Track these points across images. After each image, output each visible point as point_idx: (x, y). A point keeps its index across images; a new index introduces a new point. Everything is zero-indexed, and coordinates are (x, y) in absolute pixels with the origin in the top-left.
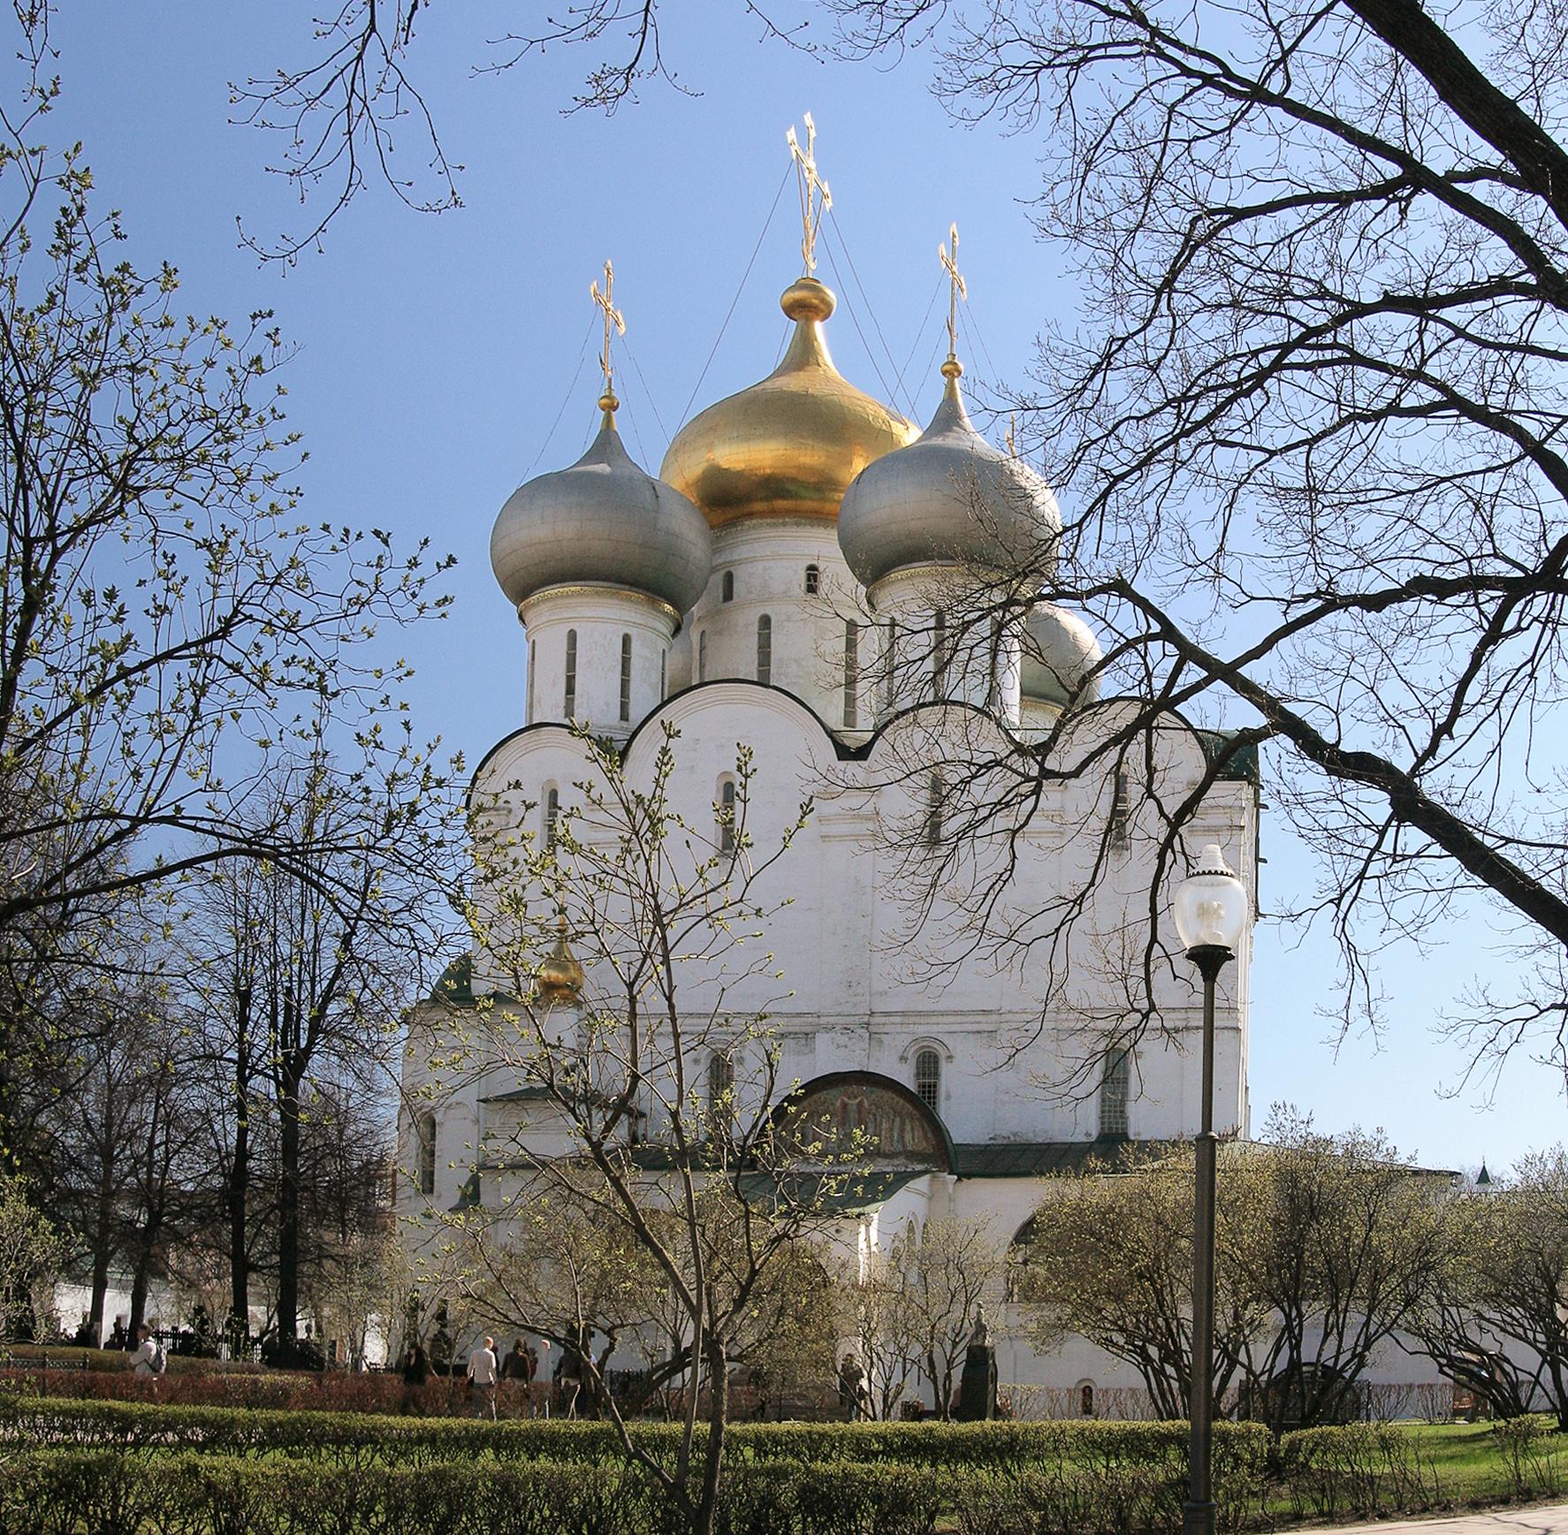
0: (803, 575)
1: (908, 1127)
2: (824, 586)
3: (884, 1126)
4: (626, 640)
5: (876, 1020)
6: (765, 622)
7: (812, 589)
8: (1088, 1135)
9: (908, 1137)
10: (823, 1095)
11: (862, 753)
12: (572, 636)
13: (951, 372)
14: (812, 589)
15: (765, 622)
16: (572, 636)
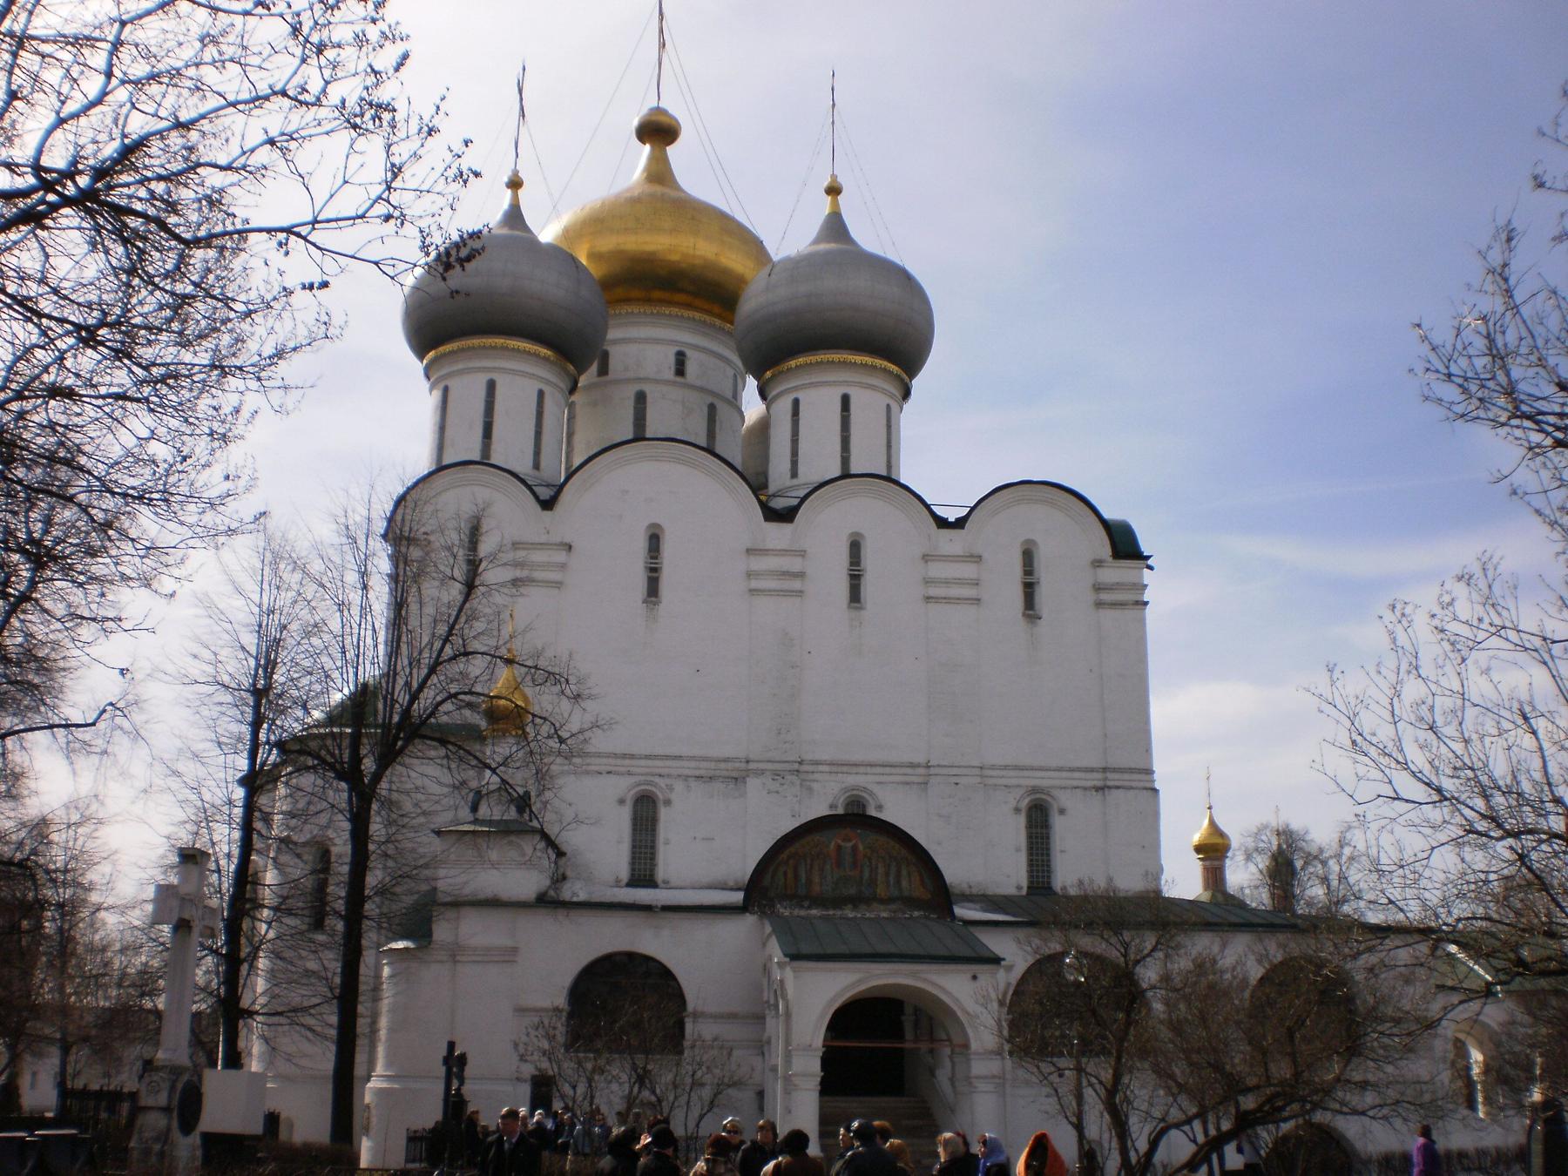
0: (672, 360)
1: (904, 872)
2: (691, 368)
3: (881, 870)
4: (541, 394)
5: (804, 768)
6: (641, 398)
7: (680, 370)
8: (1019, 888)
9: (904, 883)
10: (816, 837)
11: (786, 516)
12: (491, 386)
13: (834, 190)
14: (680, 370)
15: (641, 398)
16: (491, 386)
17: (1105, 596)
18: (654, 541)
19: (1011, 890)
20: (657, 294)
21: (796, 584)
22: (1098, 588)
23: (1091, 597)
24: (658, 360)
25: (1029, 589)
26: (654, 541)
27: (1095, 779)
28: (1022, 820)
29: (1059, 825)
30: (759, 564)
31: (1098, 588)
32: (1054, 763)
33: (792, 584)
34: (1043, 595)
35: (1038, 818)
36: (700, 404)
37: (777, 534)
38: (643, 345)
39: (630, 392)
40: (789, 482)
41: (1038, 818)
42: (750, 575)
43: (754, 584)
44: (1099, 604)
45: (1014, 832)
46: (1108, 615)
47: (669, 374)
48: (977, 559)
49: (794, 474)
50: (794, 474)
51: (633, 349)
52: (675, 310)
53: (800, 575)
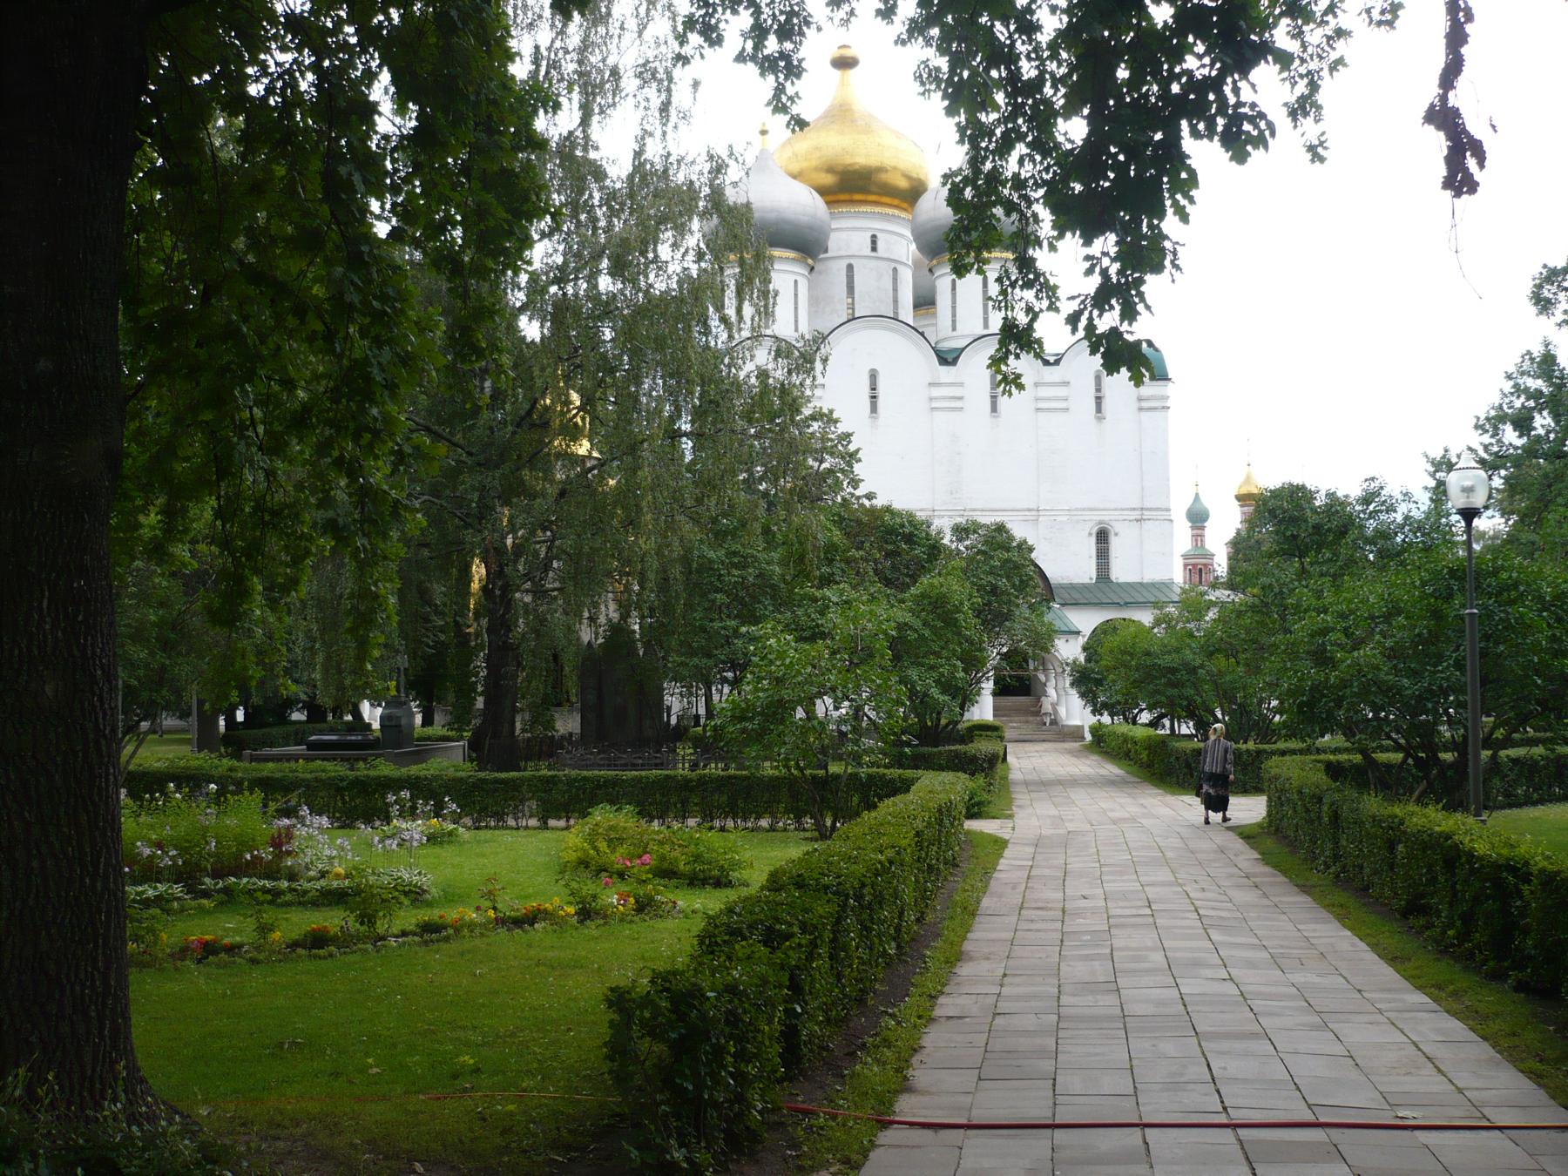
6: (850, 268)
7: (874, 249)
11: (954, 362)
14: (874, 249)
15: (850, 268)
17: (1145, 404)
18: (873, 376)
19: (1086, 581)
20: (857, 197)
21: (958, 404)
22: (1140, 399)
23: (1136, 405)
24: (861, 242)
25: (1099, 400)
26: (873, 376)
27: (1136, 515)
28: (1093, 539)
29: (1114, 543)
30: (936, 392)
31: (1140, 399)
32: (1113, 506)
33: (956, 404)
34: (1107, 404)
35: (1103, 537)
36: (887, 268)
37: (946, 373)
38: (849, 234)
39: (843, 264)
40: (950, 333)
41: (1103, 537)
42: (931, 399)
43: (935, 405)
44: (1141, 409)
45: (1091, 546)
46: (1145, 416)
47: (867, 251)
48: (1066, 384)
49: (954, 329)
50: (954, 329)
51: (843, 235)
52: (869, 209)
53: (961, 398)
